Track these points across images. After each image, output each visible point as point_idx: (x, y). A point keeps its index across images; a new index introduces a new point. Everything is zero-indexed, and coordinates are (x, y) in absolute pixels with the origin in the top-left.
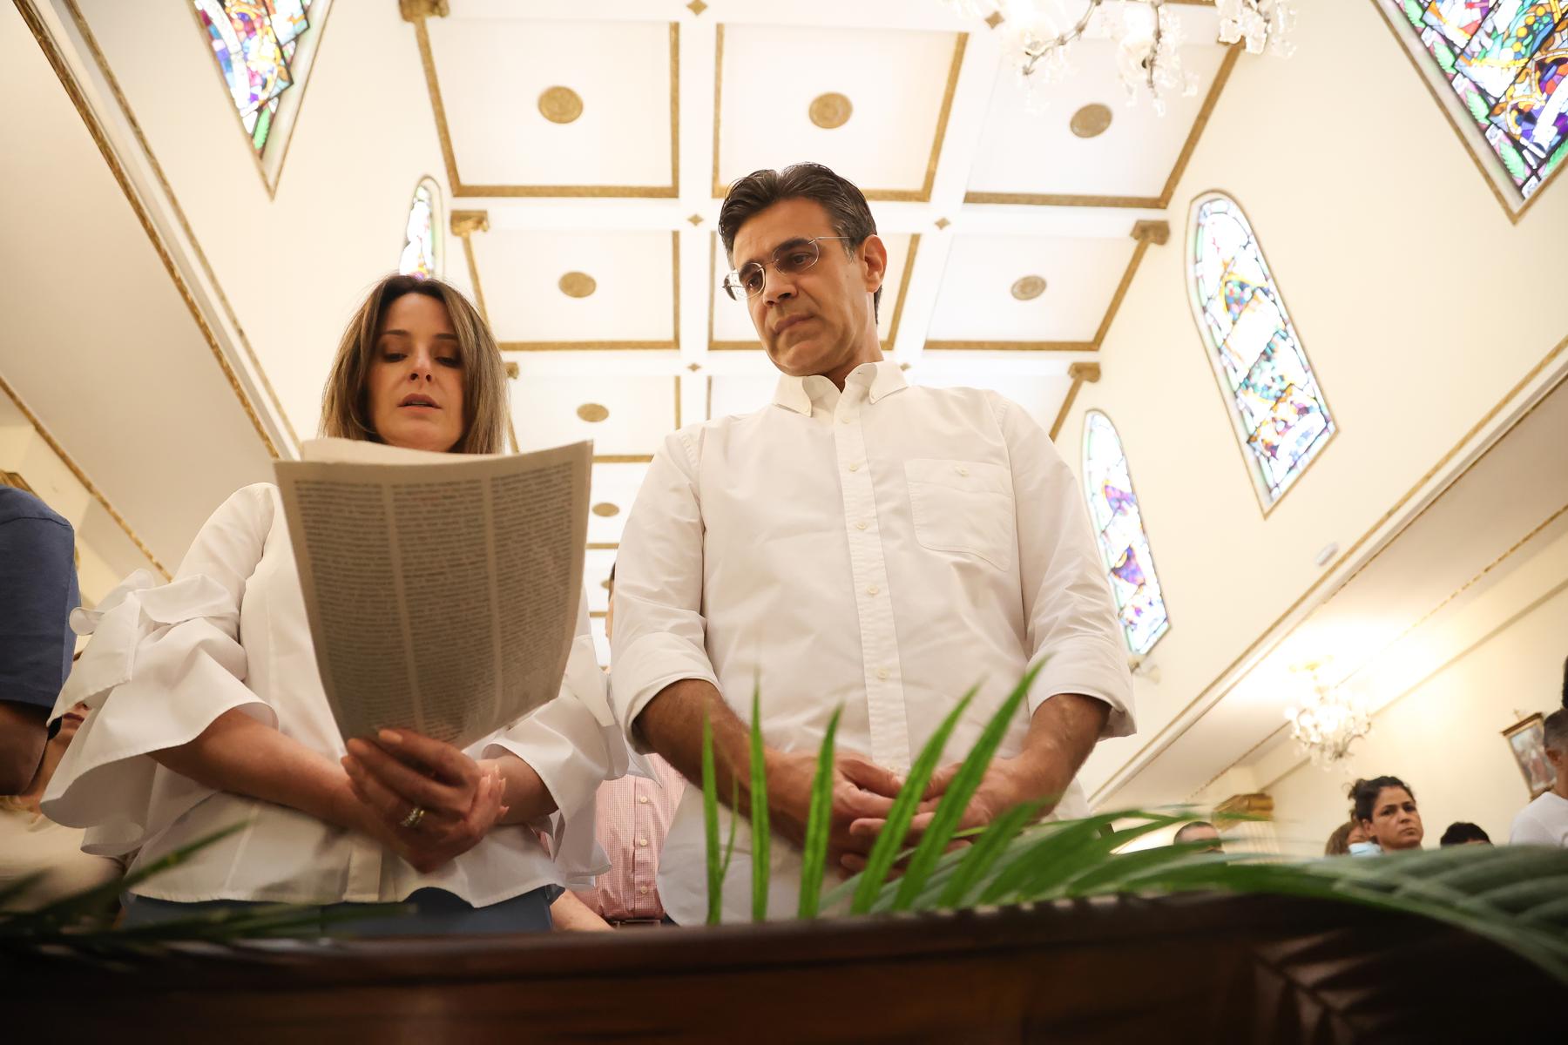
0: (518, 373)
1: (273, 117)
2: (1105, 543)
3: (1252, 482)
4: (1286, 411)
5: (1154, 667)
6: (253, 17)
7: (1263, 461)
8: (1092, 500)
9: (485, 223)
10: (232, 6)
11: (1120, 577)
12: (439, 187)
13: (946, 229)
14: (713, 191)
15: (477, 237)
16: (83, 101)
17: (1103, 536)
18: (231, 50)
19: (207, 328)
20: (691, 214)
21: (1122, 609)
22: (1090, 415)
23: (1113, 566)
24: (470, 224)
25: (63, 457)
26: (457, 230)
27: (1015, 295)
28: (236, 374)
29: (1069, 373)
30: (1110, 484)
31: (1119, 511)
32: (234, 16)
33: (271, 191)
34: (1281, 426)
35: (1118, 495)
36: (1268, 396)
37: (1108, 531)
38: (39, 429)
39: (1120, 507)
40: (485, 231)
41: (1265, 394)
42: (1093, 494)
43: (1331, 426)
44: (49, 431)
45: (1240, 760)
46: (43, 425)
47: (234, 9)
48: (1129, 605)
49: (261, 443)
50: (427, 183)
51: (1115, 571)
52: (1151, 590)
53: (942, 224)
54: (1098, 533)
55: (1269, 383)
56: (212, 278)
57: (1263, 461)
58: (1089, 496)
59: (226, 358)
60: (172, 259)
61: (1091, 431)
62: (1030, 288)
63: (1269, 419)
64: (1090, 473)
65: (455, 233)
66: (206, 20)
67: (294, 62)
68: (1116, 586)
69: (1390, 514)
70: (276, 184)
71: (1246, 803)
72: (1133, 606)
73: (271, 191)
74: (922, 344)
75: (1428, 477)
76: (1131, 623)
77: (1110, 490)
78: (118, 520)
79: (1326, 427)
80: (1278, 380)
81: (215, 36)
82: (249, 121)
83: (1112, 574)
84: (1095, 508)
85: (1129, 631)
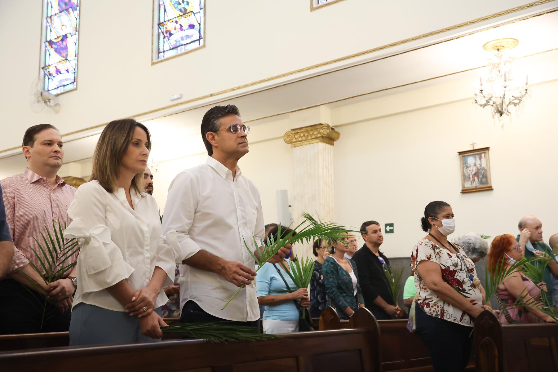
3: (152, 44)
4: (185, 22)
5: (57, 105)
7: (162, 36)
11: (52, 47)
21: (49, 65)
34: (178, 26)
36: (177, 7)
41: (176, 5)
43: (202, 41)
45: (79, 160)
51: (51, 43)
52: (71, 64)
55: (181, 1)
57: (162, 36)
63: (174, 20)
69: (211, 95)
71: (74, 182)
72: (56, 67)
75: (233, 90)
79: (199, 40)
80: (185, 3)
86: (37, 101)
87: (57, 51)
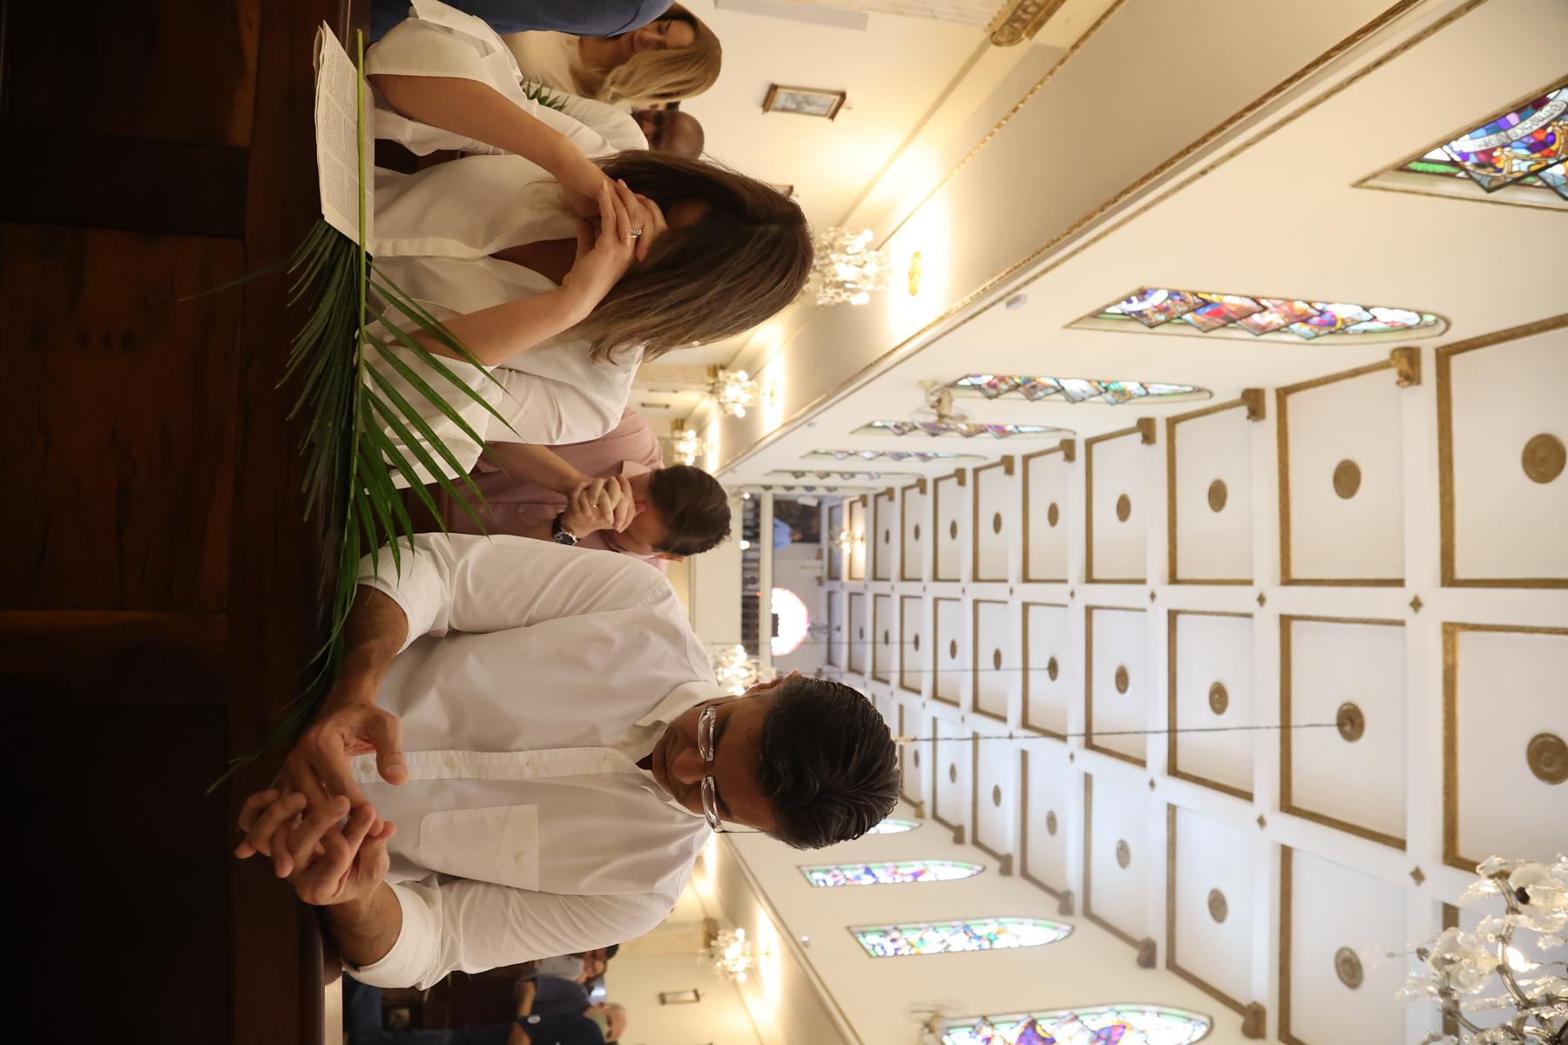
0: (1254, 421)
1: (1452, 176)
2: (1064, 1017)
6: (1554, 148)
8: (1112, 1009)
9: (1406, 383)
10: (1560, 127)
11: (1026, 1028)
12: (1441, 334)
13: (1412, 881)
14: (1452, 624)
15: (1392, 375)
16: (1387, 20)
17: (1071, 1016)
18: (1510, 132)
19: (1203, 143)
20: (1423, 600)
21: (992, 1025)
22: (1205, 1019)
23: (1040, 1022)
24: (1405, 367)
25: (1098, 23)
26: (1397, 354)
27: (1340, 952)
28: (1167, 170)
29: (1255, 1004)
30: (1127, 1032)
31: (1096, 1037)
32: (1550, 130)
33: (1361, 183)
35: (1114, 1038)
37: (1077, 1025)
39: (1099, 1038)
40: (1398, 383)
42: (1118, 1013)
47: (1557, 128)
48: (995, 1031)
49: (1111, 196)
50: (1442, 325)
51: (1032, 1024)
53: (1418, 875)
54: (1077, 1012)
56: (1248, 144)
58: (1118, 1008)
59: (1180, 162)
60: (1259, 109)
61: (1190, 1020)
62: (1350, 969)
64: (1143, 1012)
65: (1394, 351)
66: (1539, 102)
67: (1521, 188)
68: (1018, 1022)
70: (1371, 188)
73: (1361, 183)
74: (1288, 843)
76: (978, 1033)
77: (1121, 1030)
78: (1051, 73)
81: (1523, 114)
82: (1438, 154)
83: (1029, 1020)
84: (1103, 1013)
85: (970, 1029)
86: (926, 1016)
87: (1022, 1035)
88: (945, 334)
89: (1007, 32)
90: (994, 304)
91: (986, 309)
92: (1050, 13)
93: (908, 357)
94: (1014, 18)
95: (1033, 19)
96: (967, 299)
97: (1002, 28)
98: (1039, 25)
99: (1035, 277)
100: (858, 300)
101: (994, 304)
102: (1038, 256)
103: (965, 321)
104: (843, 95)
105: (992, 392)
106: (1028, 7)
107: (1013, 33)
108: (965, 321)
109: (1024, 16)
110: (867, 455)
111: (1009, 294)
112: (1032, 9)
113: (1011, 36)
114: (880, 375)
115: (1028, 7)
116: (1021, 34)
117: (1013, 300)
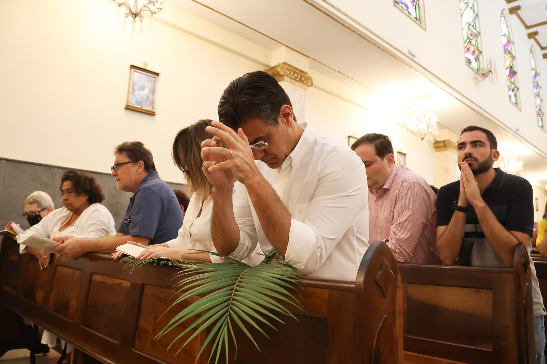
28: (328, 13)
38: (287, 46)
44: (290, 46)
46: (288, 45)
49: (348, 30)
88: (439, 79)
89: (307, 82)
90: (416, 62)
91: (420, 65)
92: (297, 69)
93: (458, 92)
94: (301, 81)
95: (299, 74)
96: (418, 73)
97: (305, 84)
98: (301, 71)
99: (396, 49)
100: (435, 120)
101: (416, 62)
102: (385, 50)
103: (429, 72)
104: (349, 137)
105: (477, 52)
106: (295, 77)
107: (307, 80)
108: (429, 72)
109: (299, 77)
110: (538, 101)
111: (408, 57)
112: (296, 75)
113: (308, 80)
114: (473, 103)
115: (295, 77)
116: (307, 77)
117: (411, 56)
